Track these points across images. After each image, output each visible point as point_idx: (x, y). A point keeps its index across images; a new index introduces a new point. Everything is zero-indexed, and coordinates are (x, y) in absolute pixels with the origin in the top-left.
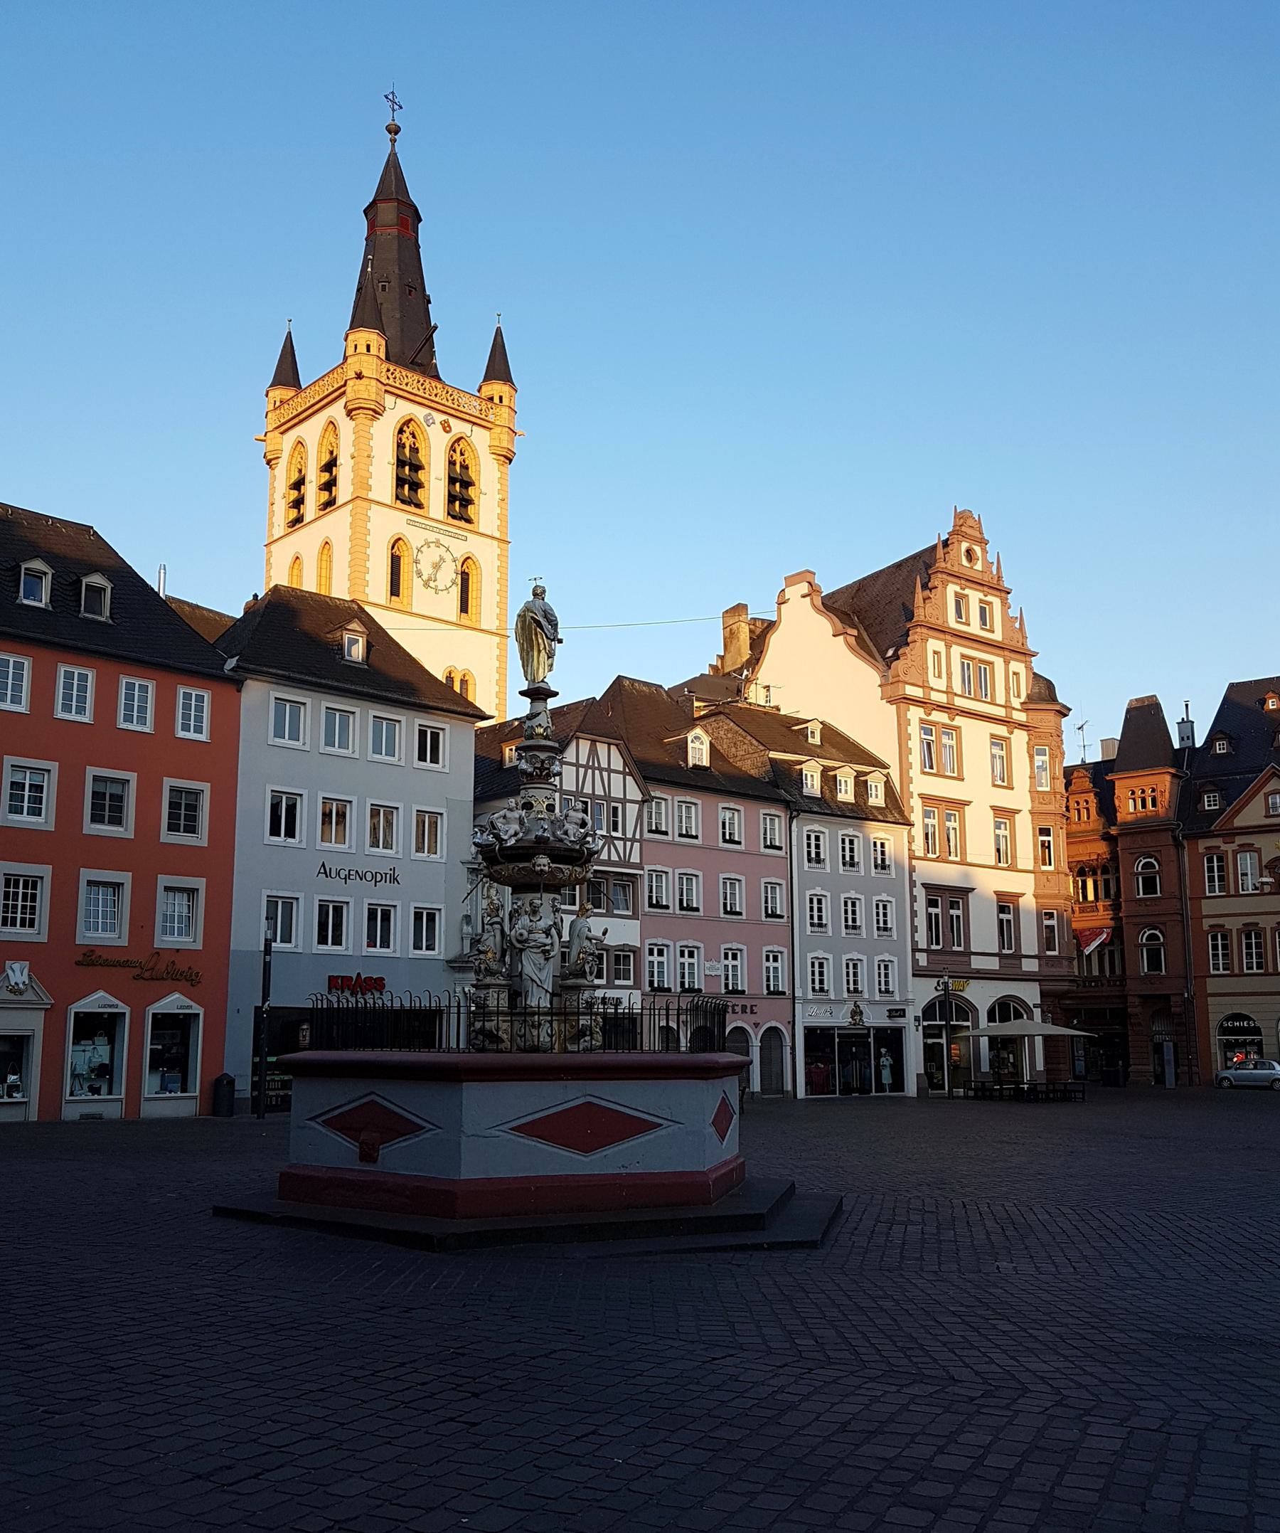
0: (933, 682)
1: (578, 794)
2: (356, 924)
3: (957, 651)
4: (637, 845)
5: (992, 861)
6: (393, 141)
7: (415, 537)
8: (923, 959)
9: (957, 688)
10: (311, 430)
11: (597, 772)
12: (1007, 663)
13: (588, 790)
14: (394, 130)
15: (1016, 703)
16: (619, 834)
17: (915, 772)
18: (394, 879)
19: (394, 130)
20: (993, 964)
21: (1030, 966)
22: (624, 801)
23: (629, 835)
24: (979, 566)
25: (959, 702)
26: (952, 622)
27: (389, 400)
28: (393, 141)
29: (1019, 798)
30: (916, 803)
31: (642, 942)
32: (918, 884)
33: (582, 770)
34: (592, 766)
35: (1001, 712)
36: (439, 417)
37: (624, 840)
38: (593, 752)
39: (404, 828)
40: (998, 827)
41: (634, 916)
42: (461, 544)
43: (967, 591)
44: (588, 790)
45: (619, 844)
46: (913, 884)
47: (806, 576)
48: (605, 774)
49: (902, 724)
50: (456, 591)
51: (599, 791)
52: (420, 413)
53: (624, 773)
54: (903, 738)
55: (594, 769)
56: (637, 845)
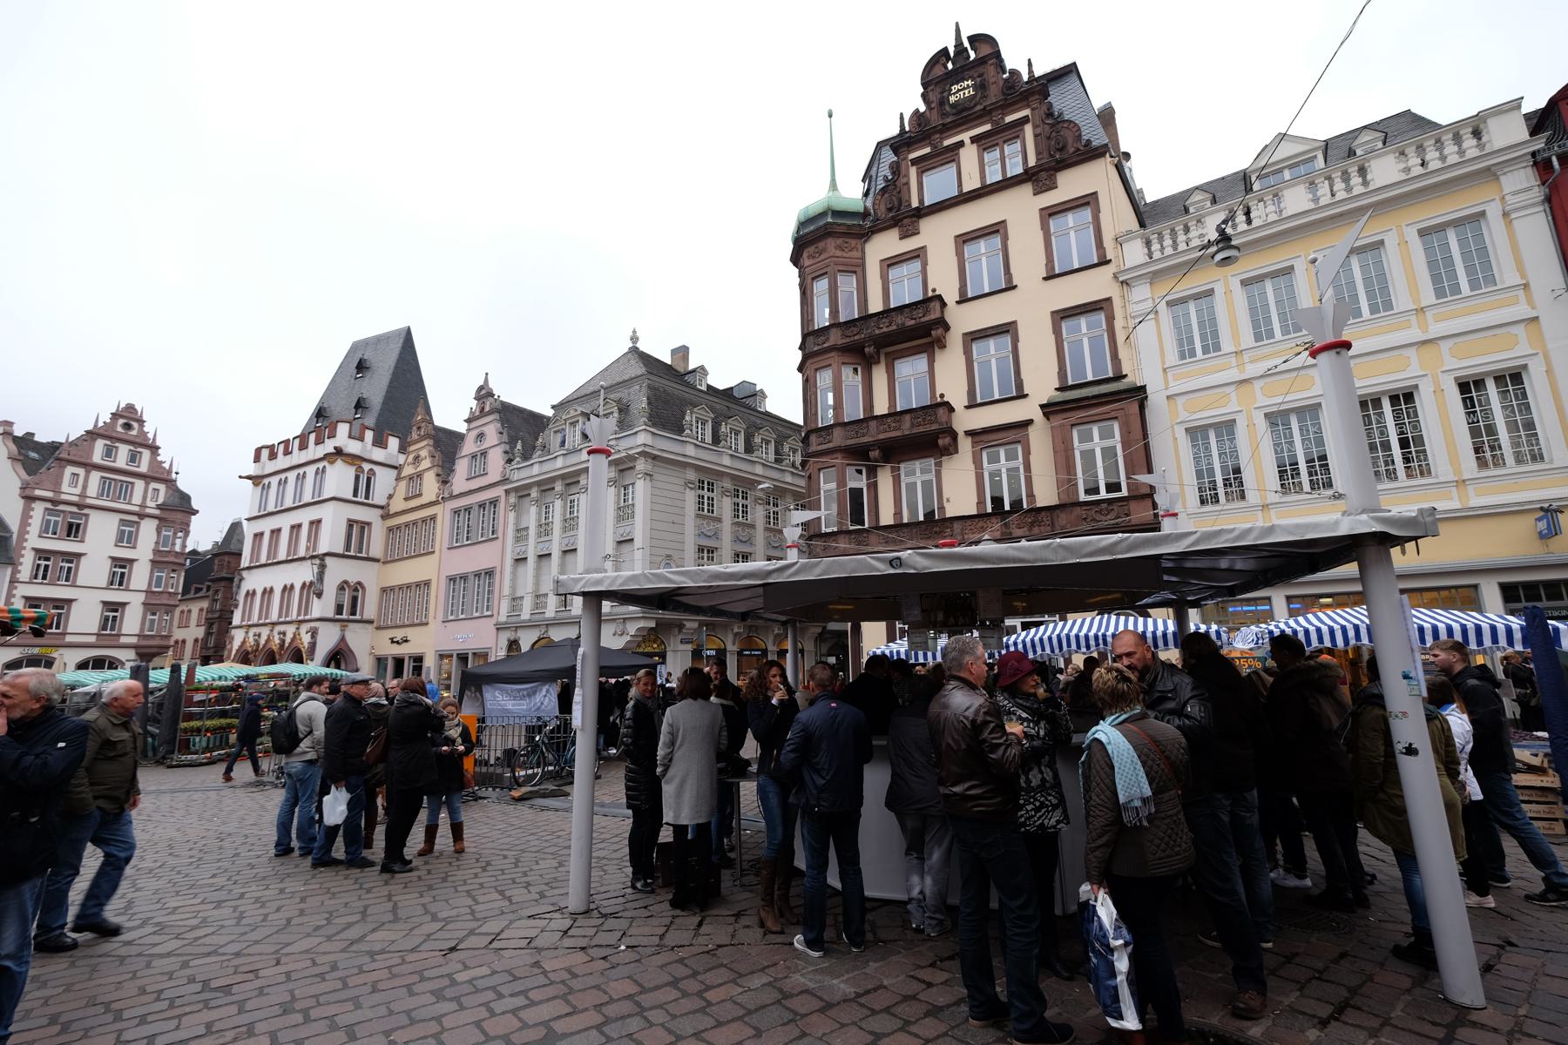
0: (65, 487)
3: (95, 476)
12: (147, 484)
15: (153, 504)
20: (93, 639)
21: (134, 640)
24: (134, 433)
25: (89, 501)
26: (97, 458)
35: (136, 509)
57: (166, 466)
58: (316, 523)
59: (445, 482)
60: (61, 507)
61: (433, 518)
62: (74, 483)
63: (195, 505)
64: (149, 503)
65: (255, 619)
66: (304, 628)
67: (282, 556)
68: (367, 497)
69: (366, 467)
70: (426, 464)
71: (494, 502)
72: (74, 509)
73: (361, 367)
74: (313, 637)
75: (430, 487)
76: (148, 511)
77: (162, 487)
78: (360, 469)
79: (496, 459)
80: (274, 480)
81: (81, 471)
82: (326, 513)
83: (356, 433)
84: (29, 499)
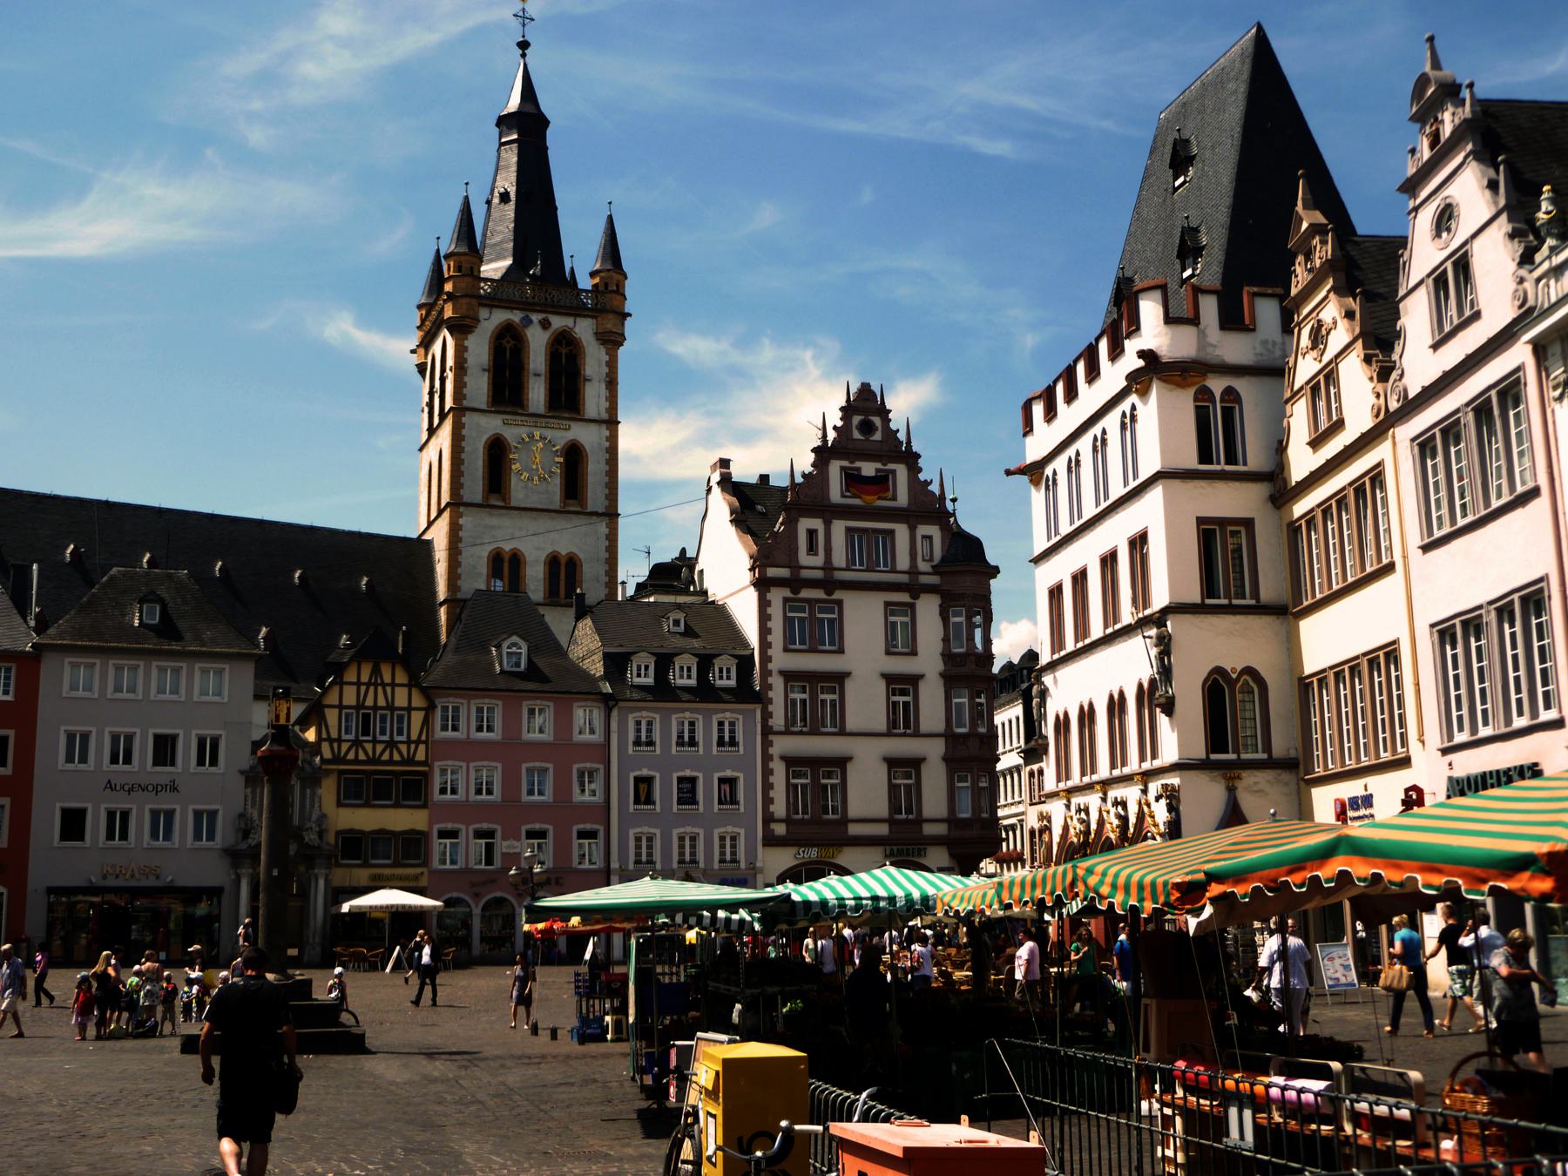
0: (804, 558)
1: (359, 706)
2: (139, 825)
3: (839, 527)
4: (422, 747)
5: (883, 727)
6: (524, 56)
7: (513, 433)
8: (780, 829)
9: (839, 559)
10: (437, 348)
11: (380, 689)
12: (912, 530)
13: (369, 702)
14: (524, 45)
16: (403, 738)
17: (776, 652)
18: (174, 789)
19: (524, 45)
20: (883, 830)
21: (940, 829)
22: (409, 709)
23: (414, 736)
24: (878, 436)
25: (840, 575)
27: (484, 313)
28: (524, 56)
29: (928, 661)
30: (777, 682)
31: (431, 827)
32: (776, 758)
33: (363, 688)
34: (376, 681)
35: (904, 578)
36: (535, 317)
37: (409, 742)
38: (376, 671)
39: (186, 752)
40: (891, 692)
41: (425, 806)
42: (562, 436)
43: (858, 464)
44: (369, 702)
45: (403, 748)
46: (767, 758)
47: (725, 463)
48: (389, 689)
49: (763, 604)
50: (556, 484)
51: (381, 702)
52: (516, 317)
53: (410, 686)
54: (764, 618)
55: (376, 685)
56: (422, 747)
57: (934, 488)
58: (1139, 542)
59: (1384, 374)
60: (806, 594)
61: (1376, 476)
62: (812, 549)
63: (992, 557)
64: (923, 566)
65: (1076, 779)
66: (1154, 787)
67: (1097, 630)
68: (1231, 459)
69: (1217, 385)
70: (1339, 337)
71: (1510, 390)
72: (819, 594)
73: (1181, 159)
74: (1171, 808)
75: (1358, 396)
76: (924, 579)
77: (934, 531)
78: (1204, 394)
79: (1495, 260)
80: (1060, 464)
81: (817, 524)
82: (1150, 513)
83: (1182, 307)
84: (762, 585)
